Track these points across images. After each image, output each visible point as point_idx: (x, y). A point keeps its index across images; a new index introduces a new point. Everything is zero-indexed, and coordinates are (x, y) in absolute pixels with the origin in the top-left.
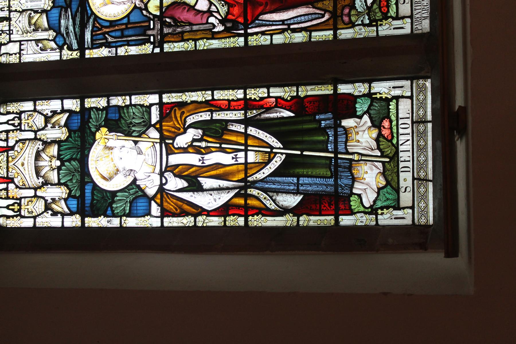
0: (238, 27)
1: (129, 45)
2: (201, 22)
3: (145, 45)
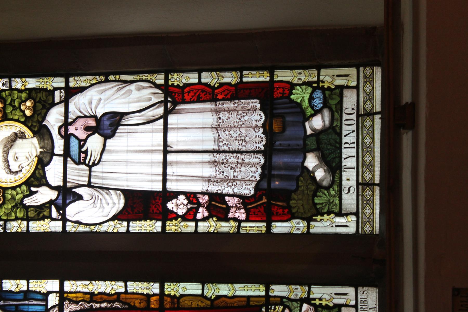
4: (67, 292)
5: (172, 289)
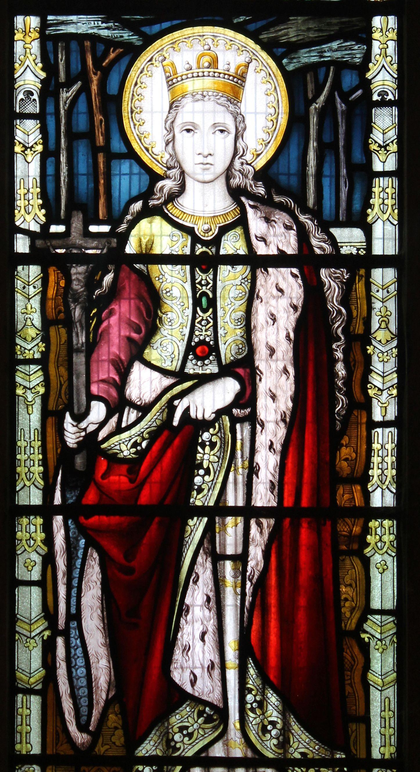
0: (73, 489)
1: (44, 156)
2: (94, 377)
3: (42, 207)
4: (368, 275)
5: (382, 535)
